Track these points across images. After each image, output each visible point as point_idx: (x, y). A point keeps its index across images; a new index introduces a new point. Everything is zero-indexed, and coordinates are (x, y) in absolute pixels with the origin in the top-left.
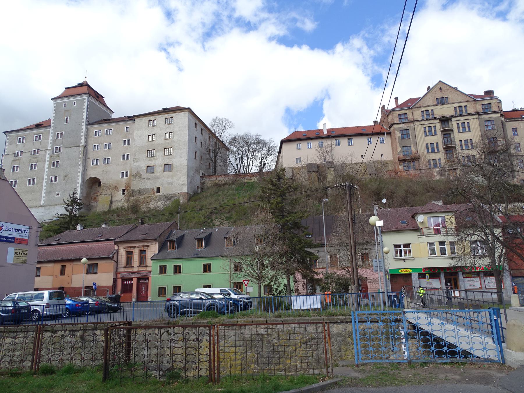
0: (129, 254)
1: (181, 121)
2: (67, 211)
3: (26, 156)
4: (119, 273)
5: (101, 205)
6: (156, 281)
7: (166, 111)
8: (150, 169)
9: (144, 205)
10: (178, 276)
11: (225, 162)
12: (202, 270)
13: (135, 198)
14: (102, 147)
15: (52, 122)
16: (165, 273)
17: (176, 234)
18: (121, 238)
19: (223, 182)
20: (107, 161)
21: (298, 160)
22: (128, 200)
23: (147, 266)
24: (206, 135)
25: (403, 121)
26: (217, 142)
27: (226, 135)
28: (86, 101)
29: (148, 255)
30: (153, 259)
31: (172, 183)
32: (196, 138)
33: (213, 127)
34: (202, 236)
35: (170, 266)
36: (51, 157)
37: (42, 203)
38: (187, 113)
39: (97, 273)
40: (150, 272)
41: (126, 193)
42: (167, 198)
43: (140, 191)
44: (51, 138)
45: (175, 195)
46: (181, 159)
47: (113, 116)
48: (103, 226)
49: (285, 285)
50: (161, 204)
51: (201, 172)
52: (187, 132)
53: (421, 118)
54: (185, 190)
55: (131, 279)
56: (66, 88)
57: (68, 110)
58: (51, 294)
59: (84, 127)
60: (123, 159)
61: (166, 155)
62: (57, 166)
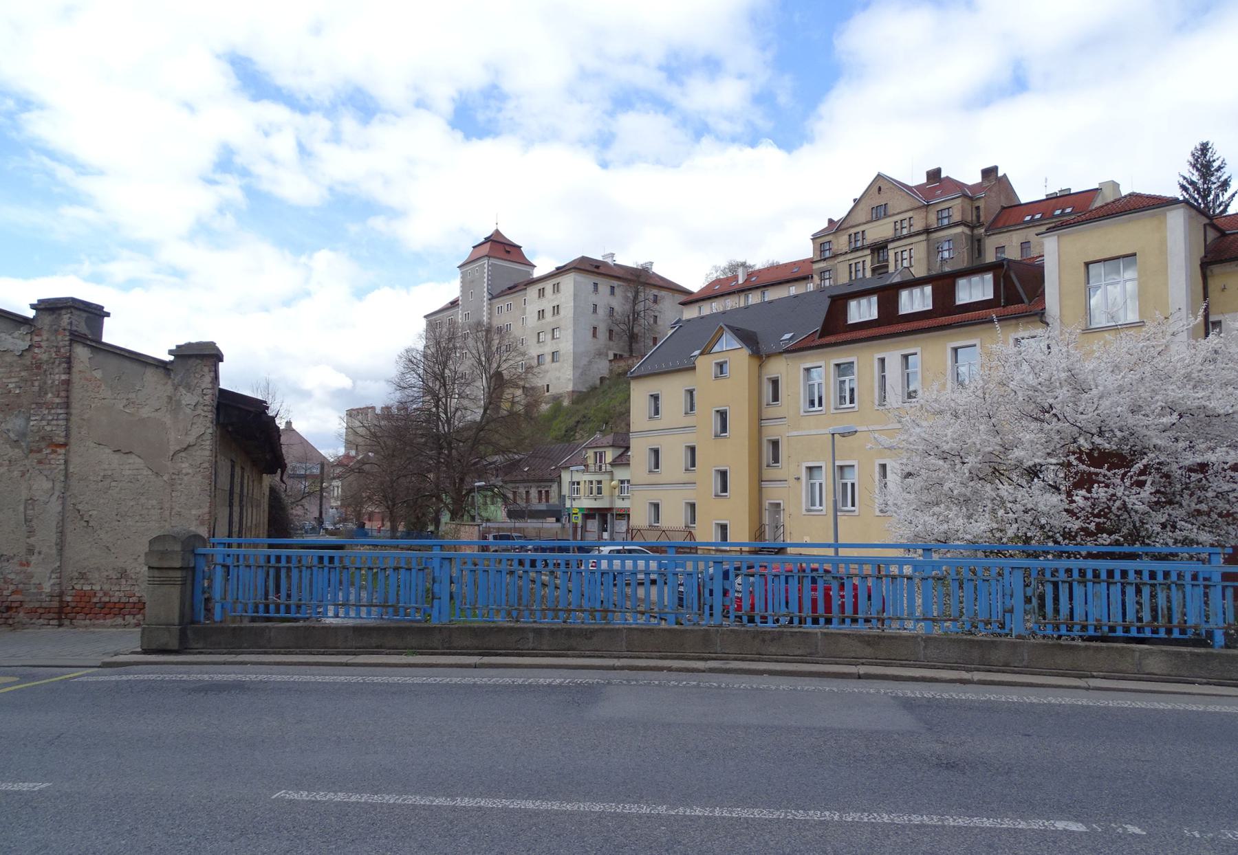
25: (827, 254)
53: (846, 249)
54: (570, 388)
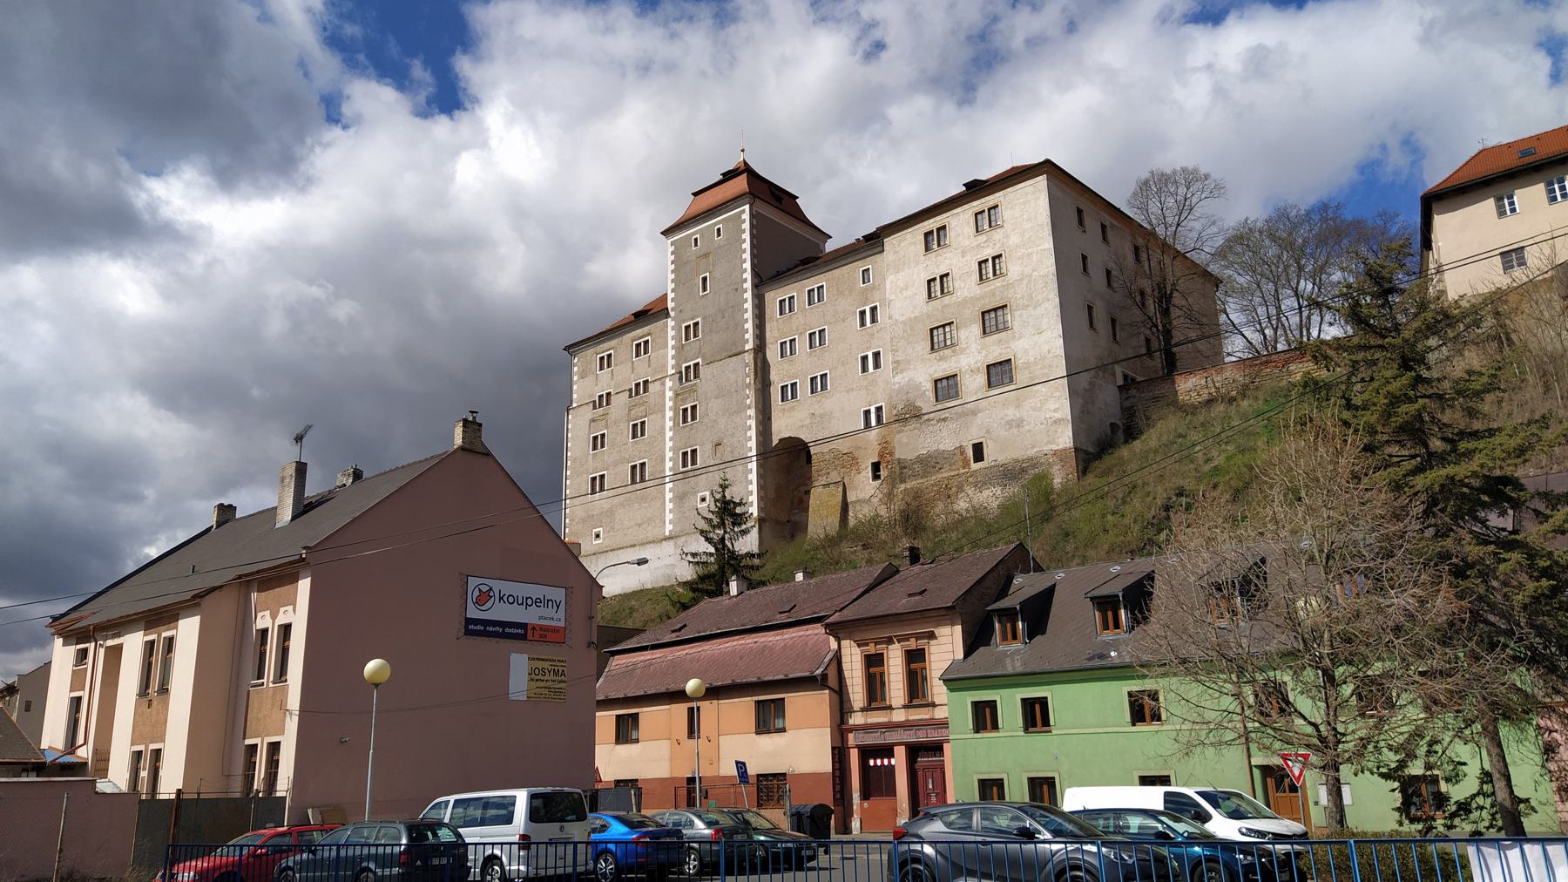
0: (874, 663)
1: (1029, 206)
2: (707, 539)
3: (621, 401)
4: (851, 731)
5: (821, 518)
6: (967, 759)
7: (976, 189)
8: (946, 387)
9: (940, 506)
10: (1038, 740)
11: (1212, 333)
12: (1128, 718)
13: (909, 485)
14: (802, 344)
15: (671, 296)
16: (995, 727)
17: (1024, 586)
18: (845, 612)
19: (1205, 397)
20: (819, 384)
21: (1512, 257)
22: (890, 496)
23: (933, 705)
24: (1122, 244)
26: (1167, 261)
27: (1197, 225)
28: (746, 216)
29: (934, 666)
30: (953, 682)
31: (1019, 423)
32: (1084, 258)
33: (1144, 208)
34: (1116, 589)
35: (1010, 703)
36: (677, 395)
37: (669, 527)
38: (1041, 182)
39: (783, 730)
40: (944, 724)
41: (883, 473)
42: (1008, 473)
43: (920, 460)
44: (671, 343)
45: (1033, 462)
46: (1040, 338)
47: (830, 246)
48: (799, 577)
49: (1486, 777)
50: (990, 497)
51: (1118, 369)
52: (1049, 244)
55: (887, 751)
56: (695, 194)
57: (706, 255)
58: (533, 797)
59: (748, 295)
60: (865, 369)
61: (992, 333)
62: (693, 418)
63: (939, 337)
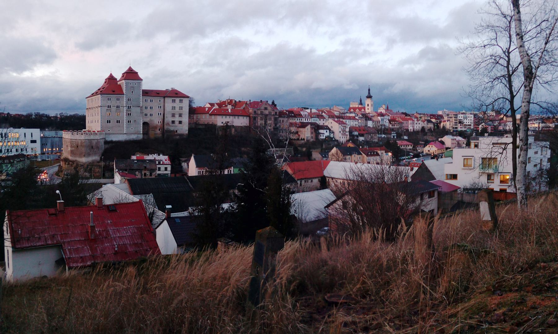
8: (173, 122)
50: (178, 137)
63: (173, 115)
